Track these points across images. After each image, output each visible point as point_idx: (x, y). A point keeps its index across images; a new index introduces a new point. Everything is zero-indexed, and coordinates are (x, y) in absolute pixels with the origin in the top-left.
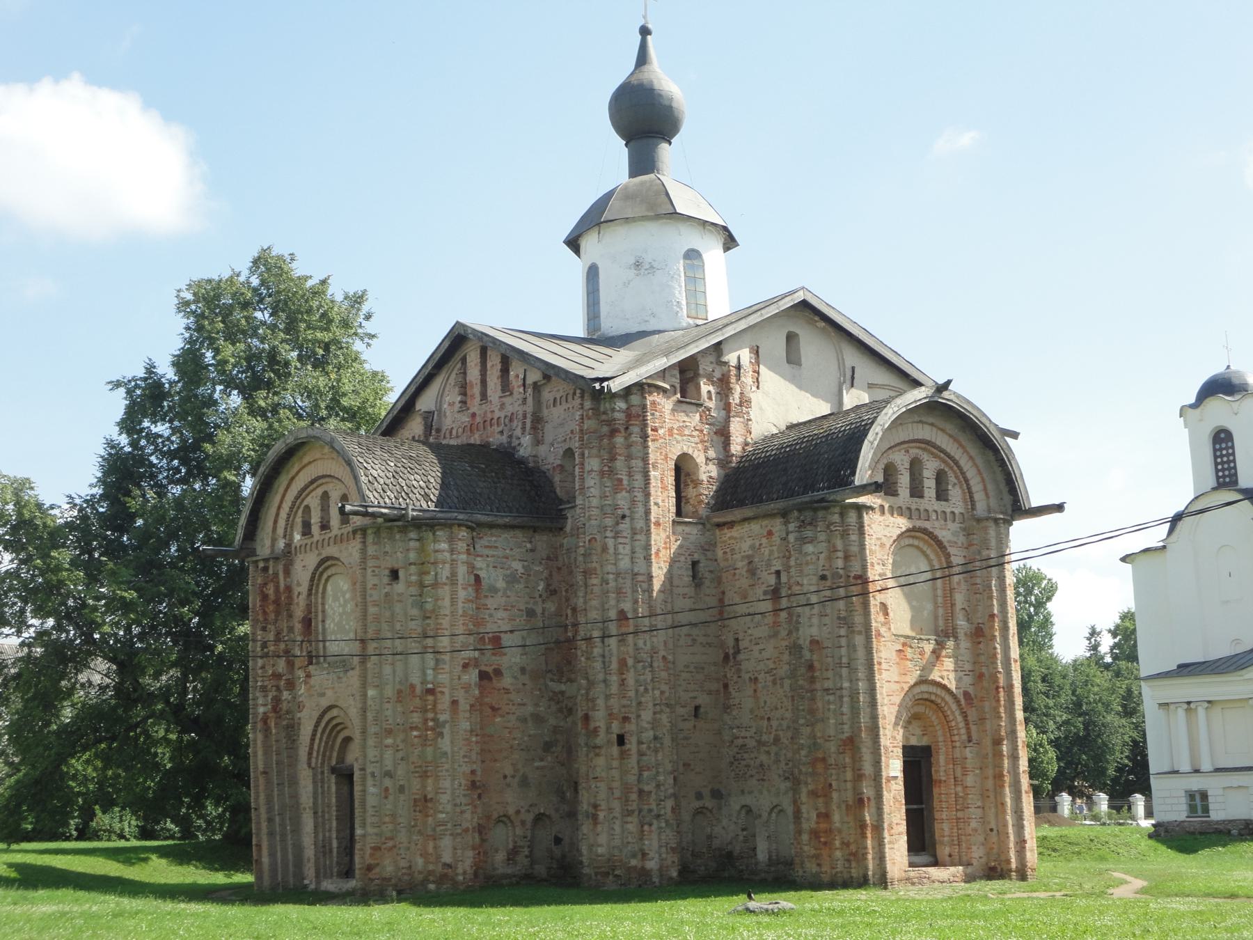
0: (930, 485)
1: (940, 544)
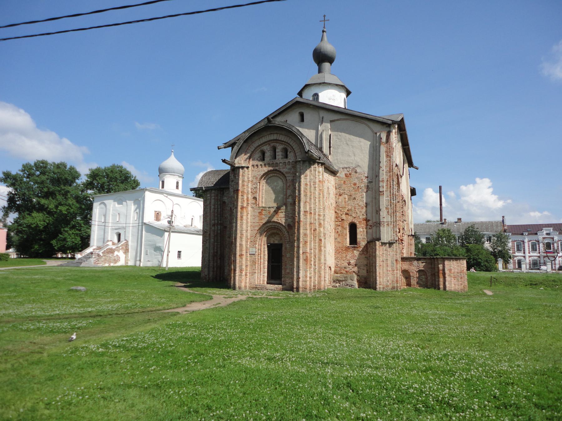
0: (279, 154)
1: (282, 173)
